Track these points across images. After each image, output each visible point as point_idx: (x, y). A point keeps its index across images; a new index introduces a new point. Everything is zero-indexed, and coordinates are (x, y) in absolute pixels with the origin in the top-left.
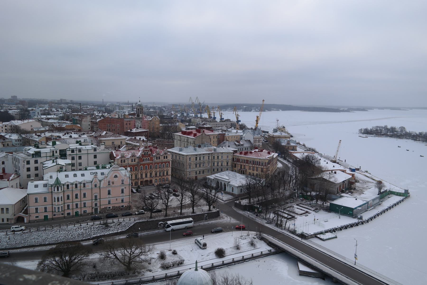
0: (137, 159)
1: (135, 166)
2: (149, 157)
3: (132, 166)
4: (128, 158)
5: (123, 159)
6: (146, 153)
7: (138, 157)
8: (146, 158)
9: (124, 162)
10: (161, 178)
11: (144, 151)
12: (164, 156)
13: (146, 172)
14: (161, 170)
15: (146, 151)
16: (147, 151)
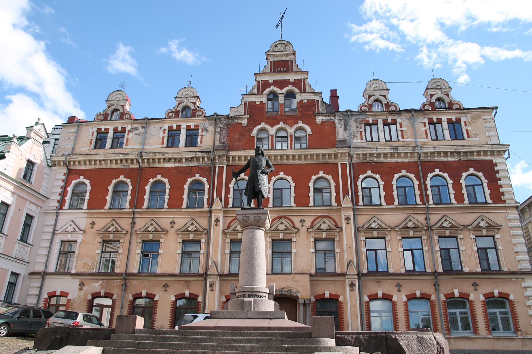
0: (211, 128)
1: (191, 172)
2: (300, 124)
3: (165, 172)
4: (147, 122)
5: (111, 126)
6: (281, 99)
7: (216, 118)
8: (281, 124)
9: (117, 142)
10: (429, 289)
11: (265, 85)
12: (431, 122)
13: (282, 227)
14: (421, 218)
15: (281, 84)
16: (290, 87)
